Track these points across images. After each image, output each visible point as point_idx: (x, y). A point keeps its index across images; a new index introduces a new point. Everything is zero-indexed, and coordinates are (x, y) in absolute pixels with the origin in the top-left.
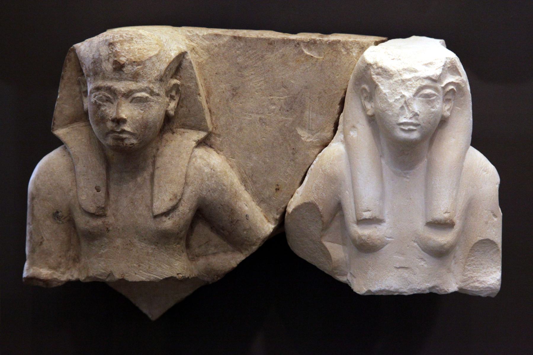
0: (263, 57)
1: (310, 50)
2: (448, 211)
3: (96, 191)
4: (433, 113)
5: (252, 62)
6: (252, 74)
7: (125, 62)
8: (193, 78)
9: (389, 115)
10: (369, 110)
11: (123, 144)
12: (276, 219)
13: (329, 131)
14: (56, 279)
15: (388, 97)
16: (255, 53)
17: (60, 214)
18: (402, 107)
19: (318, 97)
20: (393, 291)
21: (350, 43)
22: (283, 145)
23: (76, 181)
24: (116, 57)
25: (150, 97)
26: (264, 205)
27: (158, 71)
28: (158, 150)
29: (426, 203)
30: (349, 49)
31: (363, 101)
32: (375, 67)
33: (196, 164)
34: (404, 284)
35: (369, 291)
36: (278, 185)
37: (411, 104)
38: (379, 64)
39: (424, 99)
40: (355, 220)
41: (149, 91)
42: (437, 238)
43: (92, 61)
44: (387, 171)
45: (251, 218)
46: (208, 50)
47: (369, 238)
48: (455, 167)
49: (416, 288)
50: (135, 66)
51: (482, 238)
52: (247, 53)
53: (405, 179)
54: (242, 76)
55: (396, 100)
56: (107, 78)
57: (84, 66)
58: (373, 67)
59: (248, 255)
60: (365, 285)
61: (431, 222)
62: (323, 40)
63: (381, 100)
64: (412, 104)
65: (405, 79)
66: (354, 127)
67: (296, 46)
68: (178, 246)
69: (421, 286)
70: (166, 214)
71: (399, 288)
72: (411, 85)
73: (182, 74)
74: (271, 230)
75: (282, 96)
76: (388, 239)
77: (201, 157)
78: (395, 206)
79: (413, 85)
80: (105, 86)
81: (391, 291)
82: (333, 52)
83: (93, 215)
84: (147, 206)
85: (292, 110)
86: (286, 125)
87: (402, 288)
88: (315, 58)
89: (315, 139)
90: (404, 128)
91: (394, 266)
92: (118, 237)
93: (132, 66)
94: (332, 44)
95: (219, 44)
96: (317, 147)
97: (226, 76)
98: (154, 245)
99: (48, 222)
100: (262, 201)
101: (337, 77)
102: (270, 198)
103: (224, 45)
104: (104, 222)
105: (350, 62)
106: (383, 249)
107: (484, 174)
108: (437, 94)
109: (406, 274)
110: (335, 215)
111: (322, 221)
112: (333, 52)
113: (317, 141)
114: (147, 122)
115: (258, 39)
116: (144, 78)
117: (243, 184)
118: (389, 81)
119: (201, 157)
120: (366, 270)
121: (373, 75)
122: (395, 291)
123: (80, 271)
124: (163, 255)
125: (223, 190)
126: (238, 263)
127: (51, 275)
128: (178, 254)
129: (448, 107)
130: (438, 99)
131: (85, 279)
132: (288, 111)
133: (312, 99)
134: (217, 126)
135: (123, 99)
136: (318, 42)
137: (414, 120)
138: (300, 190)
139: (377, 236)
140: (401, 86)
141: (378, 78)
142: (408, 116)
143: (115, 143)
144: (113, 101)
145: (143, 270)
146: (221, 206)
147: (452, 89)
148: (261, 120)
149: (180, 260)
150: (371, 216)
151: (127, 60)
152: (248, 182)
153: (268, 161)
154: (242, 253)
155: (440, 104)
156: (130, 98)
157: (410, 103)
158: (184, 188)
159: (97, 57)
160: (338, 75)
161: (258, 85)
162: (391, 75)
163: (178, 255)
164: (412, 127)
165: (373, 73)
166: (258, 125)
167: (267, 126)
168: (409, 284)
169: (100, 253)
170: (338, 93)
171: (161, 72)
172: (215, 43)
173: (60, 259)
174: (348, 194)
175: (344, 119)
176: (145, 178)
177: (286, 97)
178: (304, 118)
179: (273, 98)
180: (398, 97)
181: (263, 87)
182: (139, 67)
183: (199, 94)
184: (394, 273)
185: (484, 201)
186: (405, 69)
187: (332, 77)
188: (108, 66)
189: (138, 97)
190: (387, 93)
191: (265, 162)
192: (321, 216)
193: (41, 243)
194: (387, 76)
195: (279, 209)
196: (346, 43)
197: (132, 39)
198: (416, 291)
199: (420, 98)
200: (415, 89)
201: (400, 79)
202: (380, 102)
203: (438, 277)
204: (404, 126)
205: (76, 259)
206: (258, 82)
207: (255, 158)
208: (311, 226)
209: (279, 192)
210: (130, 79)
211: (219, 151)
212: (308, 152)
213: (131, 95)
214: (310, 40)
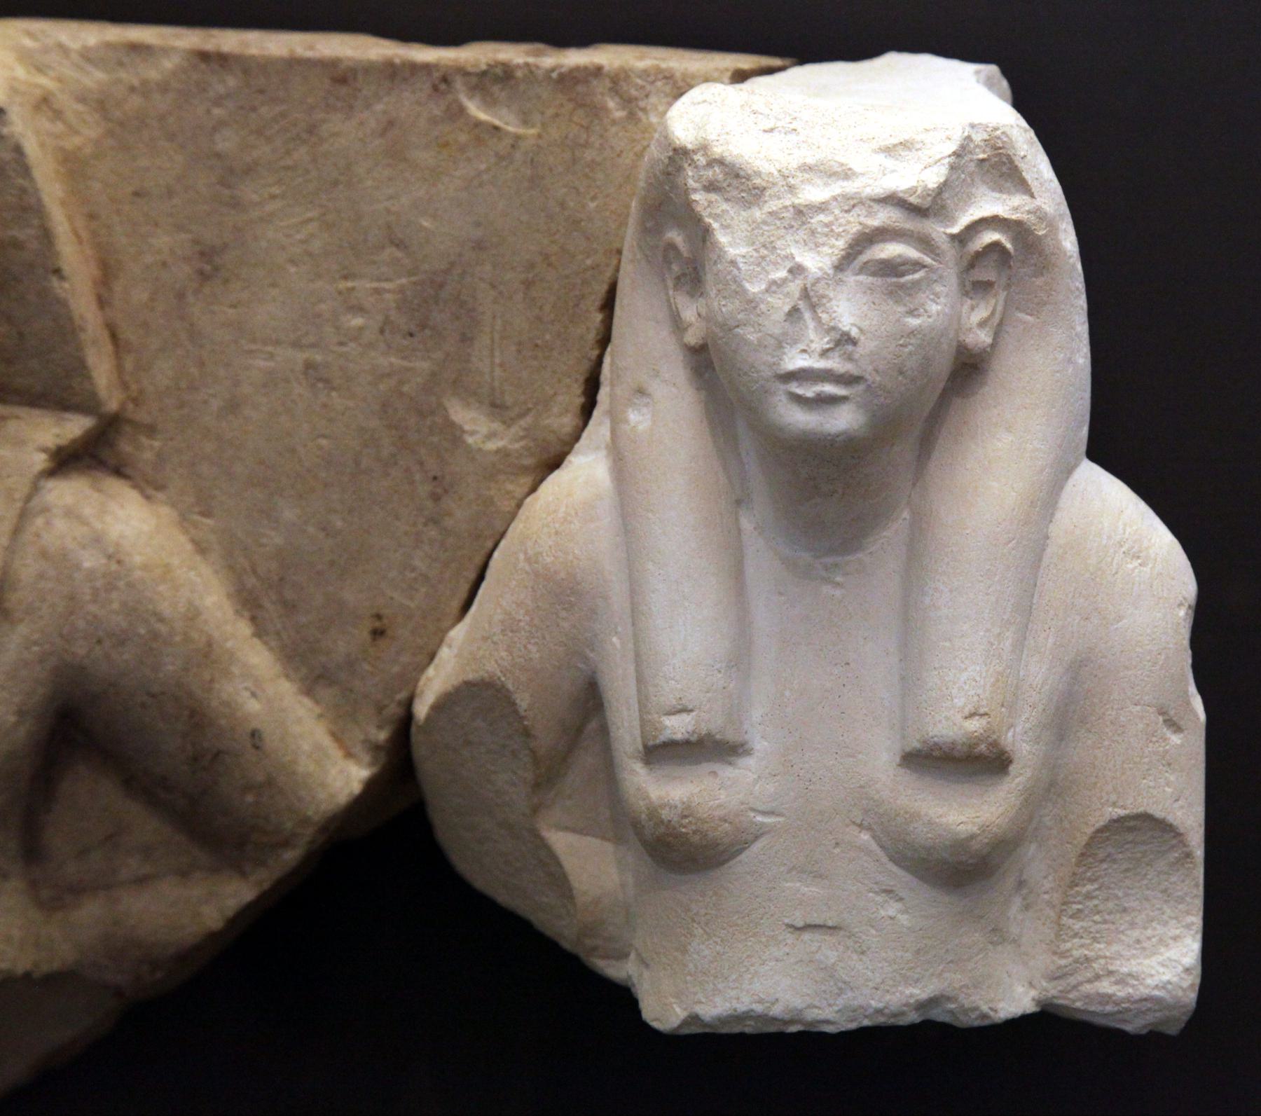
0: (312, 129)
1: (490, 102)
2: (982, 711)
4: (912, 333)
6: (273, 197)
9: (746, 342)
10: (690, 325)
13: (567, 411)
15: (743, 272)
16: (283, 115)
18: (794, 314)
19: (523, 283)
20: (780, 1017)
21: (640, 77)
22: (396, 464)
26: (327, 693)
29: (903, 678)
30: (636, 99)
31: (671, 292)
32: (700, 159)
34: (825, 991)
35: (694, 1019)
36: (379, 617)
37: (824, 301)
38: (715, 149)
39: (878, 281)
40: (641, 748)
42: (940, 811)
45: (271, 739)
46: (101, 104)
47: (686, 817)
48: (1010, 541)
49: (870, 1006)
51: (1122, 812)
52: (253, 115)
53: (826, 589)
54: (236, 204)
55: (775, 286)
58: (693, 160)
59: (266, 886)
60: (678, 995)
61: (919, 751)
62: (537, 67)
63: (720, 286)
64: (830, 300)
65: (807, 206)
66: (641, 391)
67: (435, 88)
69: (888, 997)
71: (804, 1006)
72: (827, 225)
74: (356, 788)
75: (387, 280)
76: (759, 818)
77: (69, 513)
78: (787, 693)
79: (834, 227)
81: (774, 1019)
82: (574, 109)
85: (428, 332)
86: (406, 389)
87: (816, 1007)
88: (507, 133)
89: (517, 441)
90: (800, 391)
91: (787, 921)
95: (145, 83)
96: (525, 470)
100: (320, 677)
101: (592, 205)
102: (350, 664)
103: (164, 88)
105: (638, 148)
106: (743, 857)
107: (1130, 566)
108: (928, 260)
109: (828, 950)
110: (580, 730)
111: (533, 752)
112: (574, 109)
113: (522, 447)
115: (293, 63)
117: (247, 614)
119: (69, 513)
121: (695, 190)
122: (787, 1017)
125: (155, 636)
126: (230, 913)
129: (981, 313)
130: (936, 281)
132: (411, 335)
133: (501, 288)
134: (141, 391)
136: (519, 74)
137: (837, 360)
138: (458, 633)
139: (719, 806)
140: (791, 231)
141: (710, 202)
142: (813, 346)
147: (996, 246)
148: (310, 371)
150: (694, 732)
152: (267, 604)
153: (339, 524)
154: (243, 875)
155: (942, 300)
157: (823, 296)
160: (594, 198)
161: (298, 237)
162: (758, 188)
164: (829, 389)
165: (695, 185)
167: (334, 394)
168: (840, 989)
170: (598, 266)
174: (618, 646)
175: (613, 363)
177: (404, 281)
178: (474, 359)
179: (353, 289)
180: (781, 274)
181: (316, 245)
183: (57, 271)
184: (787, 950)
185: (1127, 668)
186: (807, 168)
187: (572, 204)
190: (740, 260)
191: (325, 528)
192: (527, 733)
195: (385, 706)
196: (622, 76)
198: (866, 1017)
199: (861, 278)
200: (841, 244)
201: (788, 203)
202: (717, 295)
203: (951, 962)
204: (800, 385)
207: (289, 514)
208: (495, 772)
209: (382, 643)
212: (489, 489)
214: (489, 65)
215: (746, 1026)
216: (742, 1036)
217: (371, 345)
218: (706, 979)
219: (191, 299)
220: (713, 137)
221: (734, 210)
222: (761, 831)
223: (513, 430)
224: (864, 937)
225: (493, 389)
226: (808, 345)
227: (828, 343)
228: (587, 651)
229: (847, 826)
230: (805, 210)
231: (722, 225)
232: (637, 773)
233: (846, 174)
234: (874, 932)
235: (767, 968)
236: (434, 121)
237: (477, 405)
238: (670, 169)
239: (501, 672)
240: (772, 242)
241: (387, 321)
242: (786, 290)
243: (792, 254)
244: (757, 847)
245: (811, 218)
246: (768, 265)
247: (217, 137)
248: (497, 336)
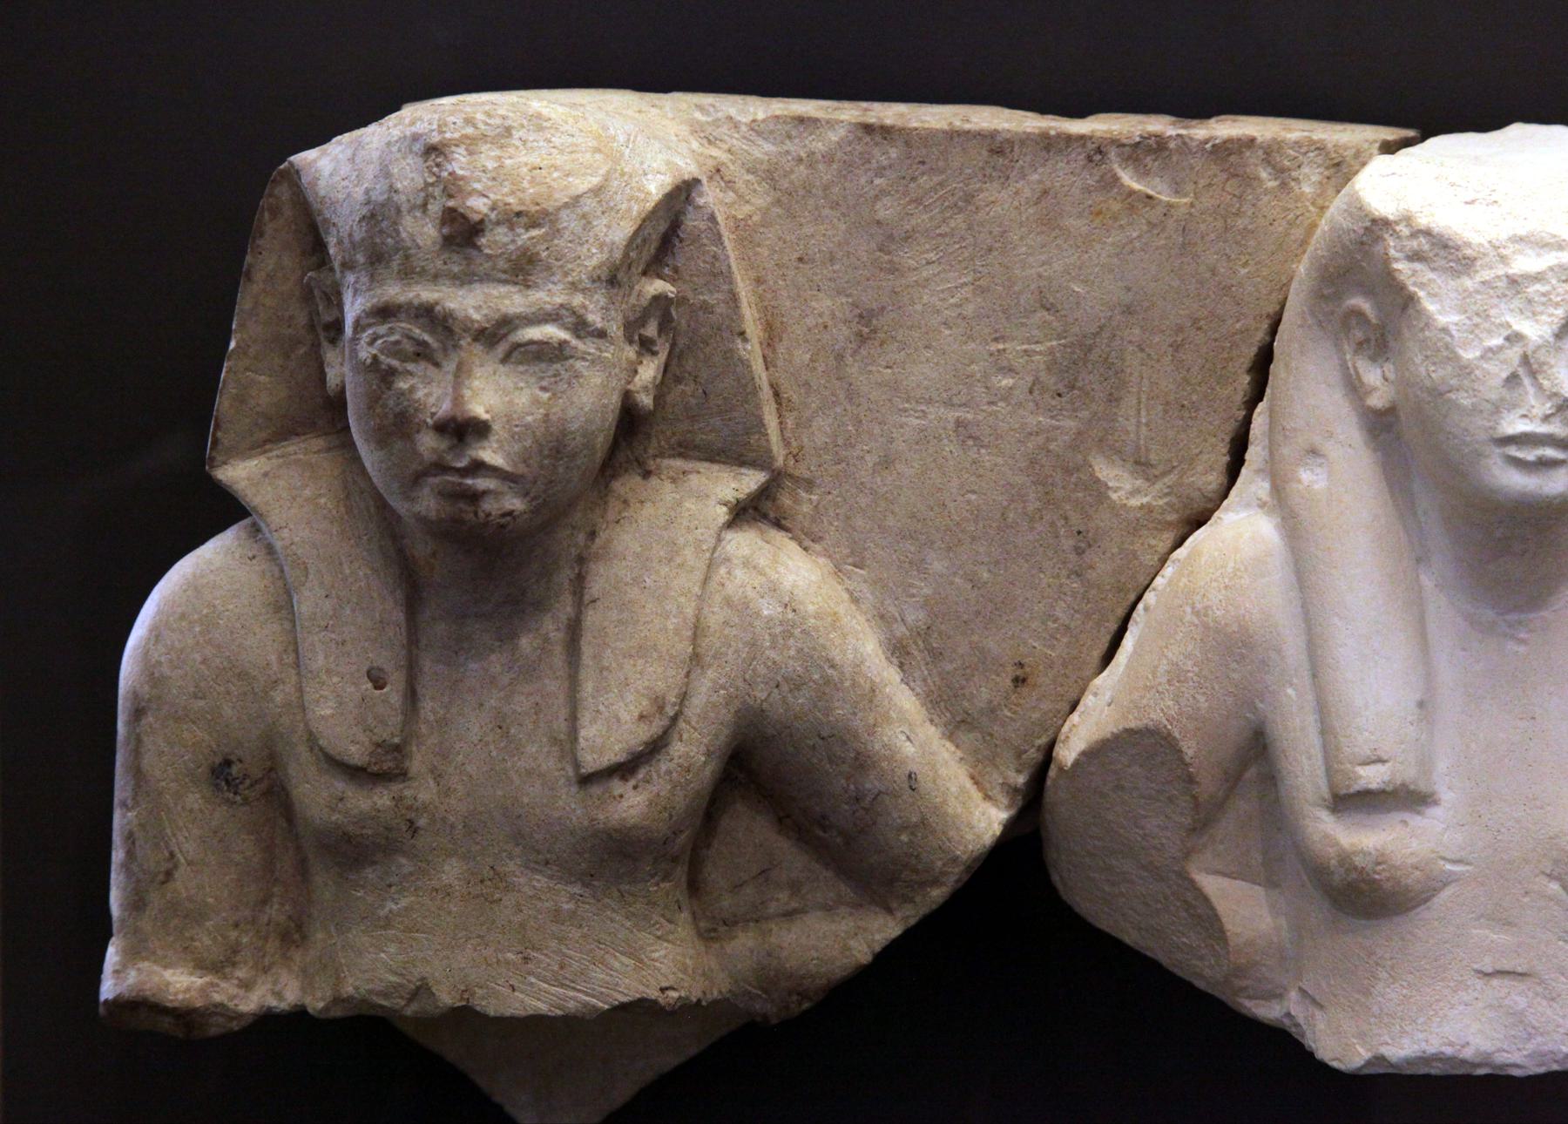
0: (969, 198)
1: (1143, 173)
3: (370, 685)
5: (931, 218)
6: (928, 263)
7: (486, 215)
8: (719, 275)
9: (1458, 406)
10: (1375, 389)
11: (476, 514)
12: (1016, 790)
13: (1212, 469)
14: (222, 1005)
15: (1456, 339)
16: (941, 184)
17: (235, 770)
18: (1513, 380)
19: (1171, 346)
20: (1470, 1060)
21: (1292, 148)
23: (296, 651)
24: (451, 196)
25: (574, 342)
26: (968, 738)
27: (601, 246)
28: (592, 535)
32: (1404, 230)
33: (730, 588)
35: (1380, 1059)
36: (1021, 665)
37: (1545, 367)
38: (1419, 220)
40: (1327, 796)
41: (570, 320)
43: (364, 211)
44: (1442, 609)
45: (925, 783)
46: (769, 174)
47: (1379, 864)
52: (912, 185)
53: (1511, 646)
54: (894, 269)
55: (1488, 354)
57: (334, 231)
58: (1394, 231)
59: (912, 922)
60: (1362, 1036)
62: (1191, 139)
63: (1429, 353)
64: (1551, 367)
65: (1522, 276)
67: (1090, 159)
68: (666, 885)
70: (625, 769)
71: (1493, 1049)
72: (1544, 295)
73: (680, 262)
74: (997, 829)
75: (1037, 342)
76: (1449, 867)
78: (1473, 746)
79: (1552, 297)
80: (410, 304)
81: (1463, 1062)
83: (358, 774)
84: (555, 741)
86: (1052, 446)
87: (1504, 1051)
88: (1161, 201)
90: (1520, 454)
91: (1476, 966)
92: (450, 855)
93: (512, 228)
94: (1224, 151)
95: (811, 154)
97: (837, 267)
98: (579, 885)
99: (194, 800)
101: (1243, 271)
102: (992, 710)
103: (829, 158)
104: (398, 800)
105: (1291, 216)
109: (1518, 996)
112: (1228, 179)
113: (1166, 504)
114: (564, 433)
115: (953, 135)
116: (553, 274)
117: (895, 661)
118: (1458, 281)
119: (746, 563)
120: (1366, 982)
121: (1397, 260)
122: (1477, 1060)
123: (306, 975)
124: (612, 921)
125: (827, 681)
126: (878, 948)
127: (203, 990)
128: (663, 916)
131: (326, 1009)
132: (1059, 395)
134: (801, 448)
135: (478, 348)
136: (1172, 145)
137: (1558, 424)
138: (1107, 681)
140: (1504, 300)
141: (1415, 272)
142: (1535, 411)
144: (439, 356)
145: (538, 978)
146: (820, 742)
149: (671, 937)
150: (1389, 782)
151: (493, 209)
153: (986, 575)
154: (890, 911)
156: (502, 348)
157: (1544, 364)
158: (688, 675)
159: (382, 198)
160: (1245, 264)
161: (952, 301)
162: (1468, 258)
164: (1550, 452)
165: (1398, 255)
166: (950, 447)
167: (983, 451)
168: (1530, 1034)
169: (382, 913)
171: (611, 251)
173: (233, 934)
176: (546, 640)
177: (1054, 343)
179: (1004, 350)
180: (1497, 341)
181: (969, 310)
182: (535, 233)
183: (742, 333)
184: (1476, 994)
187: (1222, 270)
188: (424, 231)
189: (532, 342)
190: (1453, 328)
192: (1191, 780)
193: (169, 875)
194: (1451, 264)
195: (1026, 752)
196: (1276, 147)
197: (508, 131)
198: (1556, 1061)
201: (1501, 272)
202: (1423, 361)
205: (293, 935)
206: (951, 292)
207: (938, 566)
208: (1146, 817)
209: (1024, 690)
210: (504, 276)
211: (807, 539)
212: (1132, 543)
213: (505, 336)
214: (1141, 136)
215: (1434, 1067)
216: (1427, 1077)
217: (1020, 405)
218: (1393, 1021)
220: (1414, 209)
221: (1443, 278)
222: (1450, 880)
223: (1159, 485)
224: (1554, 984)
225: (1138, 448)
226: (1528, 410)
227: (1550, 408)
228: (1257, 701)
229: (1536, 876)
230: (1520, 280)
231: (1429, 293)
232: (1322, 820)
233: (1560, 245)
234: (1563, 979)
235: (1456, 1012)
236: (1087, 190)
237: (1121, 463)
238: (1365, 238)
239: (1168, 720)
240: (1485, 311)
241: (1036, 381)
242: (1502, 356)
243: (1508, 323)
244: (1447, 893)
245: (1526, 287)
246: (1482, 332)
247: (878, 205)
248: (1144, 397)
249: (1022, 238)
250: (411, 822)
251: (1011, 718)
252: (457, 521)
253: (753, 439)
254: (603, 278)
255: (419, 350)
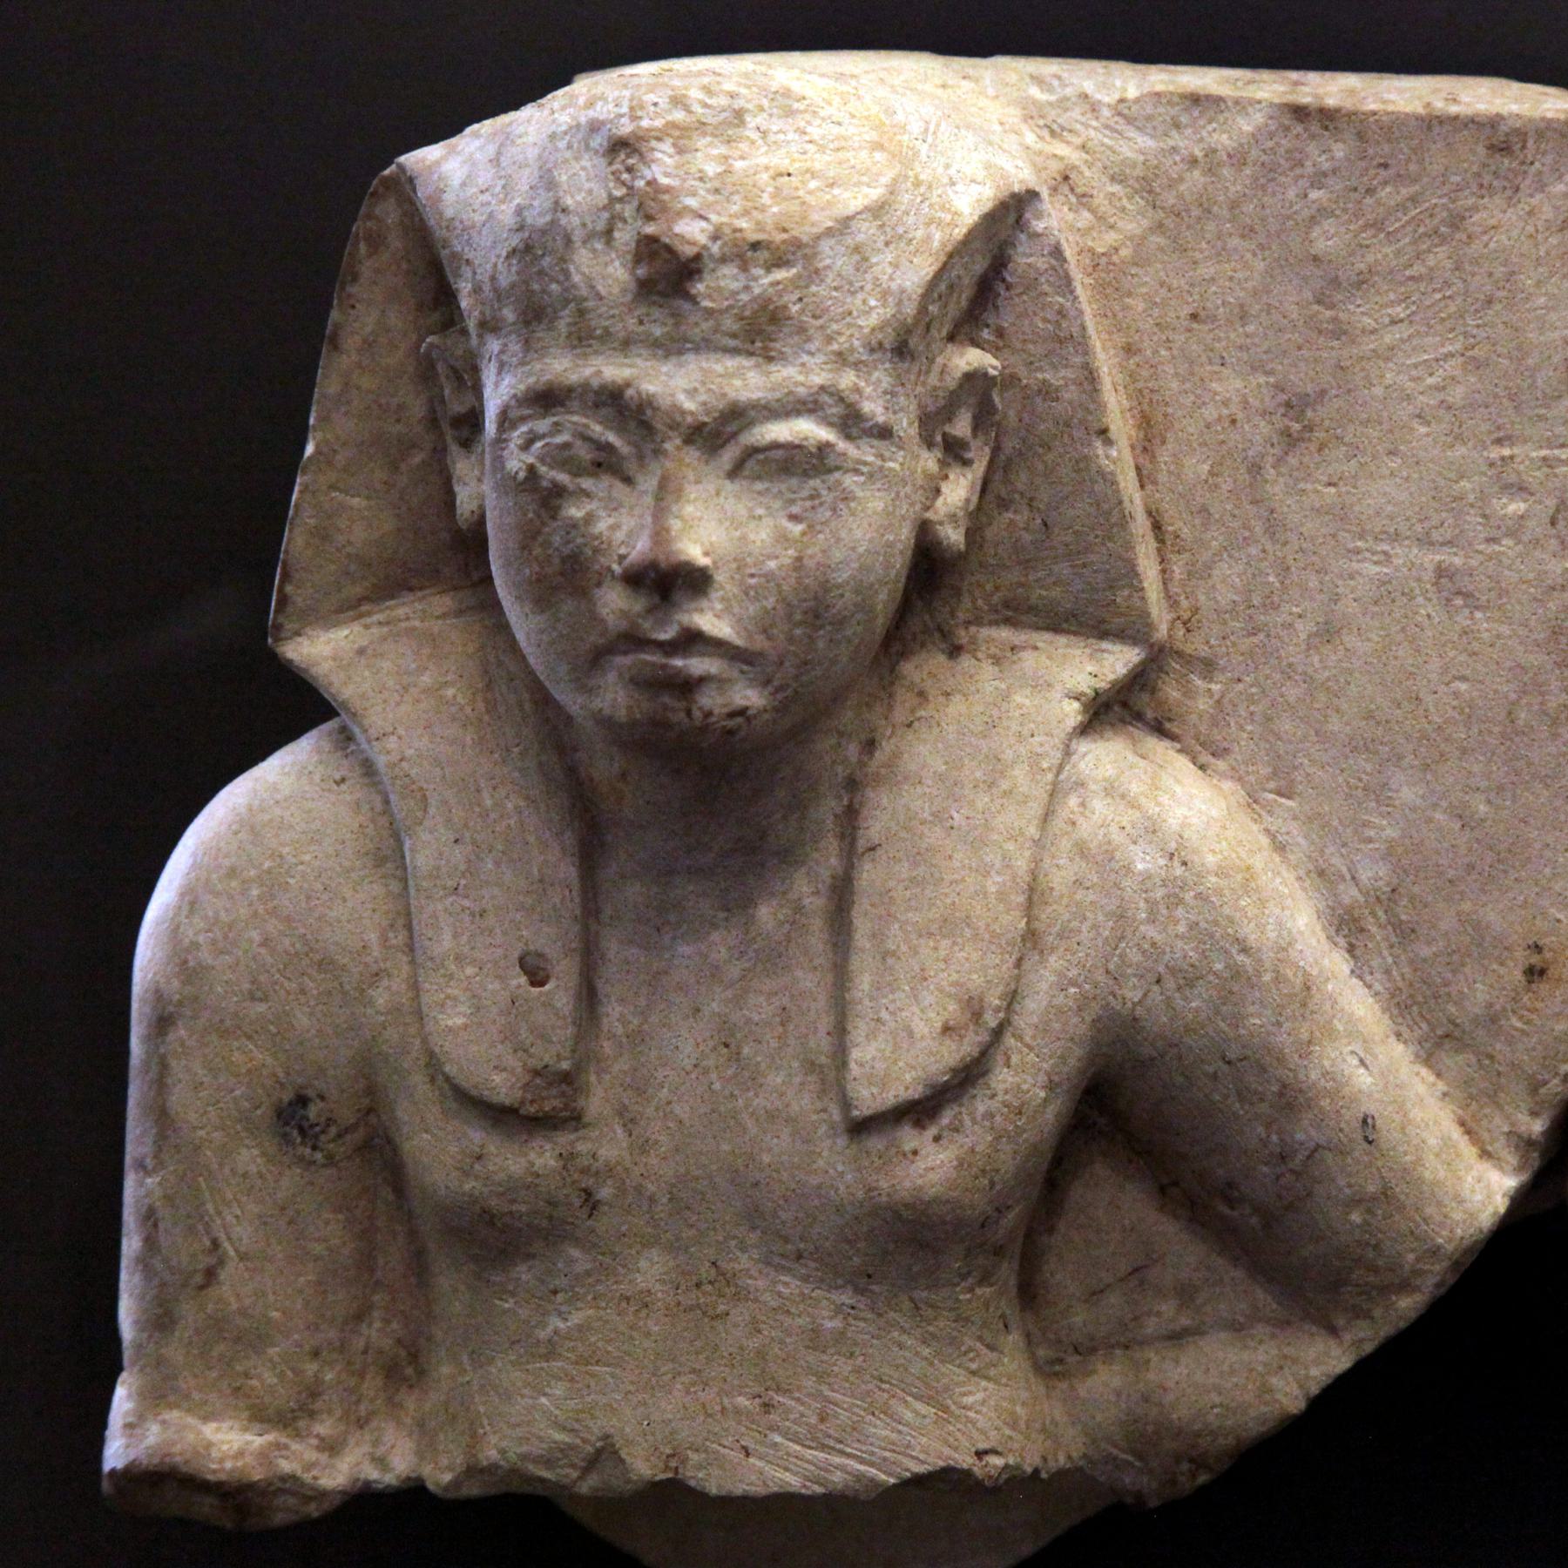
0: (1457, 221)
3: (523, 980)
5: (1398, 253)
6: (1394, 322)
7: (705, 247)
11: (689, 713)
12: (1530, 1143)
16: (1414, 199)
17: (313, 1112)
23: (409, 927)
24: (649, 218)
25: (842, 445)
26: (1454, 1061)
27: (885, 295)
28: (870, 745)
33: (1085, 829)
36: (1538, 948)
41: (836, 411)
43: (515, 241)
45: (1388, 1132)
50: (759, 271)
52: (1369, 201)
54: (1339, 332)
56: (600, 338)
57: (467, 272)
68: (985, 1291)
74: (1501, 1204)
77: (1111, 790)
80: (585, 386)
84: (811, 1066)
92: (647, 1245)
93: (744, 268)
95: (1211, 152)
97: (1250, 328)
99: (249, 1157)
102: (1492, 1019)
103: (1238, 159)
104: (568, 1158)
114: (826, 586)
115: (1432, 123)
116: (809, 340)
117: (1342, 942)
119: (1111, 790)
123: (423, 1430)
124: (901, 1346)
125: (1237, 973)
126: (1315, 1390)
128: (980, 1339)
131: (456, 1483)
134: (1196, 610)
135: (692, 455)
143: (645, 705)
144: (631, 467)
145: (785, 1435)
146: (1225, 1068)
149: (992, 1372)
151: (715, 237)
153: (1483, 808)
156: (729, 455)
158: (1019, 963)
161: (1430, 381)
163: (978, 1345)
166: (1428, 608)
167: (1478, 615)
169: (542, 1335)
171: (899, 303)
172: (1184, 142)
173: (311, 1368)
176: (799, 909)
179: (1512, 457)
181: (1457, 394)
182: (781, 275)
183: (1103, 432)
189: (776, 446)
191: (1464, 819)
193: (210, 1274)
195: (1545, 1083)
197: (739, 114)
206: (1430, 367)
207: (1408, 794)
209: (1543, 987)
210: (732, 343)
213: (734, 435)
219: (1270, 473)
249: (1539, 284)
250: (588, 1193)
251: (1523, 1032)
252: (659, 723)
253: (1121, 596)
254: (888, 346)
255: (602, 456)
